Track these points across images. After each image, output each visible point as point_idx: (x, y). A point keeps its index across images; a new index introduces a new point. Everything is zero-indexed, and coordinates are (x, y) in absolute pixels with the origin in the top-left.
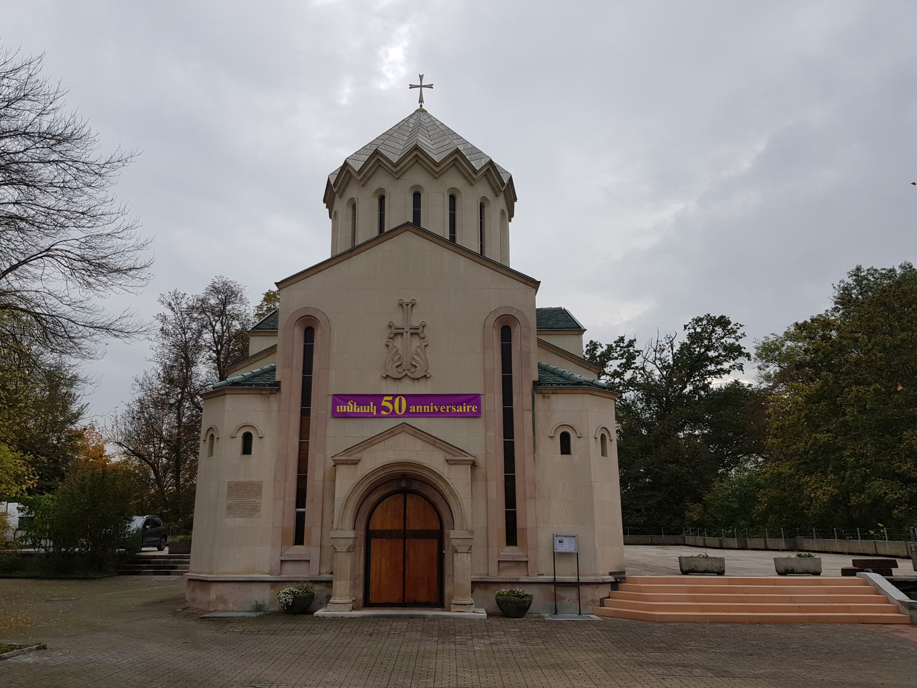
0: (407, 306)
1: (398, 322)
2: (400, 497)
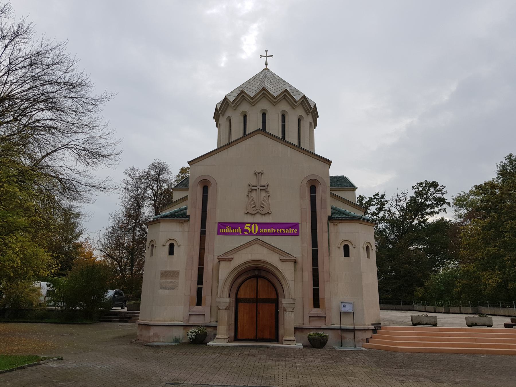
0: (259, 174)
2: (255, 280)
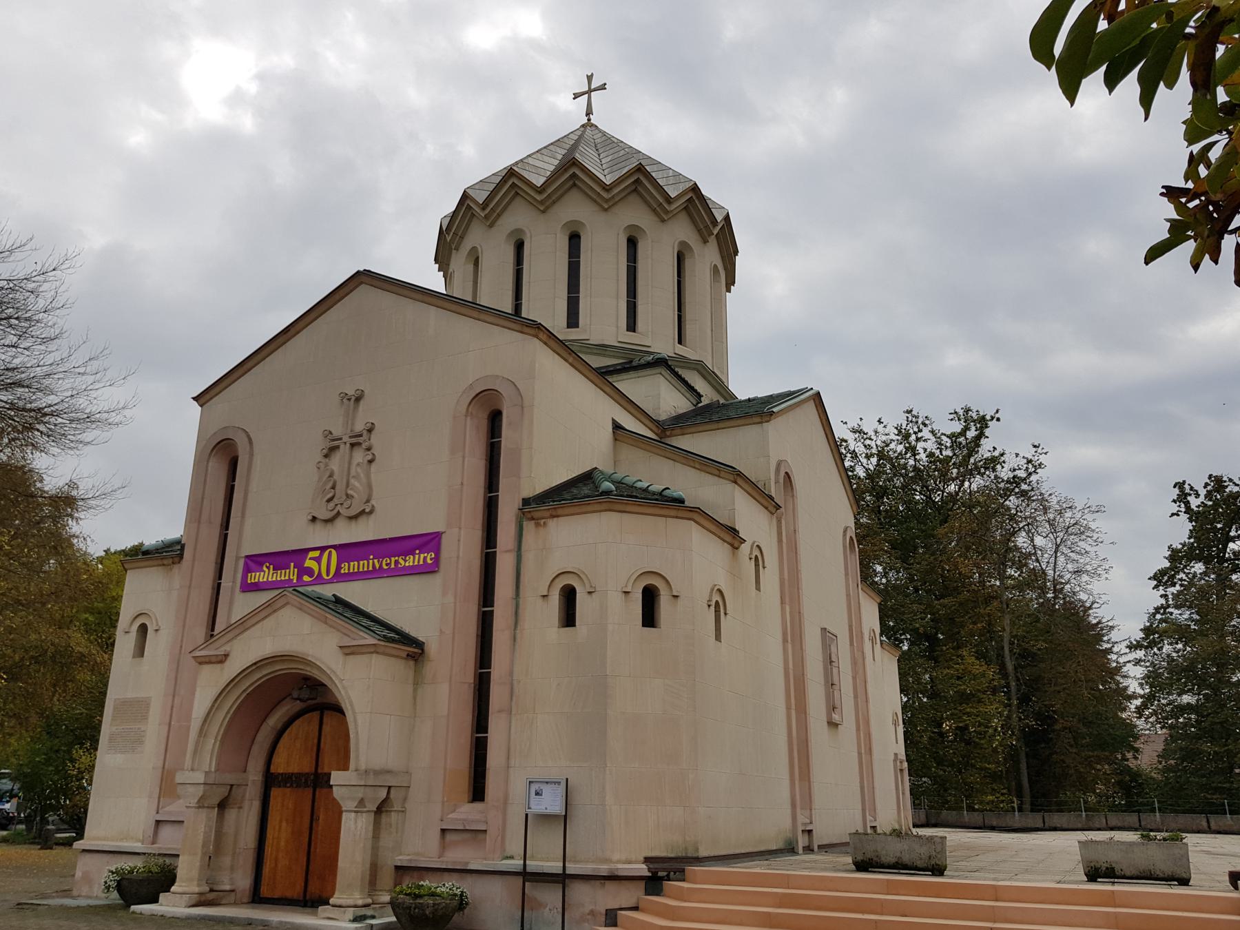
2: (316, 715)
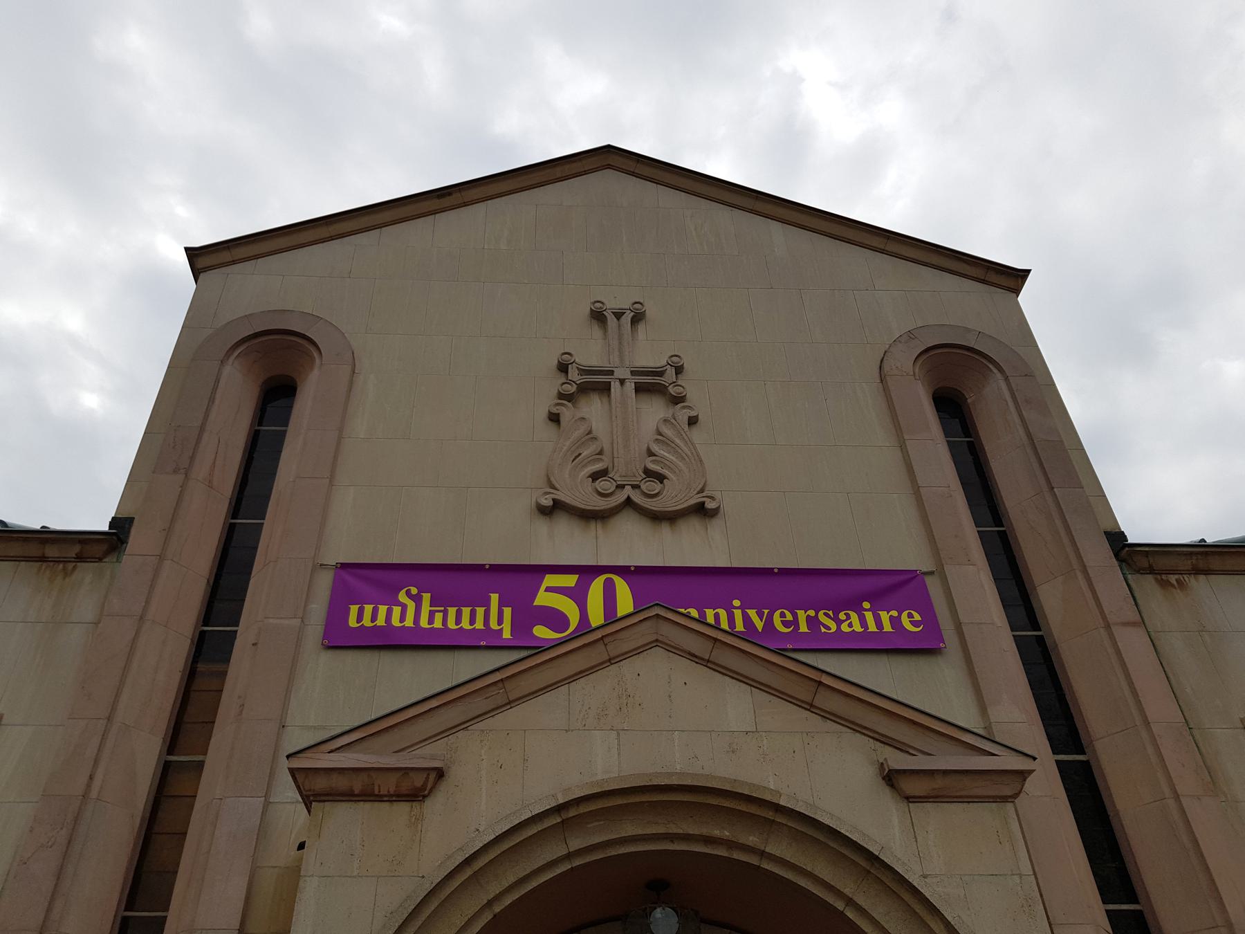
1: (591, 351)
